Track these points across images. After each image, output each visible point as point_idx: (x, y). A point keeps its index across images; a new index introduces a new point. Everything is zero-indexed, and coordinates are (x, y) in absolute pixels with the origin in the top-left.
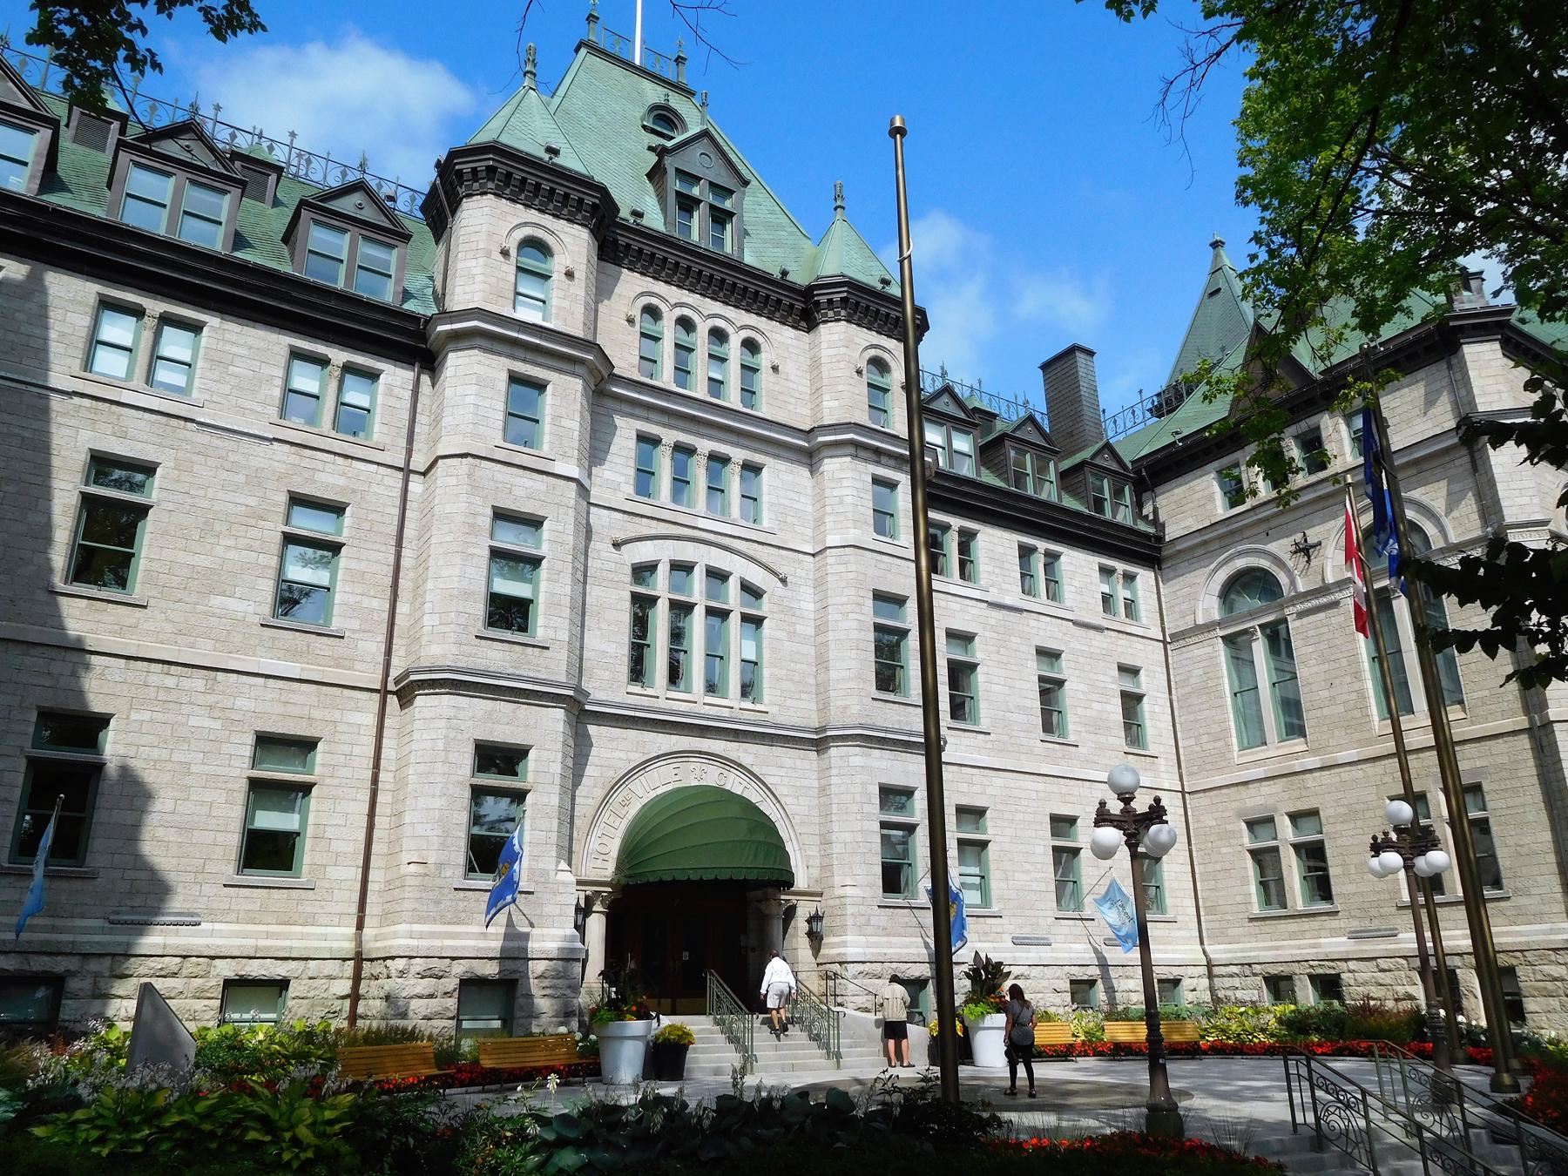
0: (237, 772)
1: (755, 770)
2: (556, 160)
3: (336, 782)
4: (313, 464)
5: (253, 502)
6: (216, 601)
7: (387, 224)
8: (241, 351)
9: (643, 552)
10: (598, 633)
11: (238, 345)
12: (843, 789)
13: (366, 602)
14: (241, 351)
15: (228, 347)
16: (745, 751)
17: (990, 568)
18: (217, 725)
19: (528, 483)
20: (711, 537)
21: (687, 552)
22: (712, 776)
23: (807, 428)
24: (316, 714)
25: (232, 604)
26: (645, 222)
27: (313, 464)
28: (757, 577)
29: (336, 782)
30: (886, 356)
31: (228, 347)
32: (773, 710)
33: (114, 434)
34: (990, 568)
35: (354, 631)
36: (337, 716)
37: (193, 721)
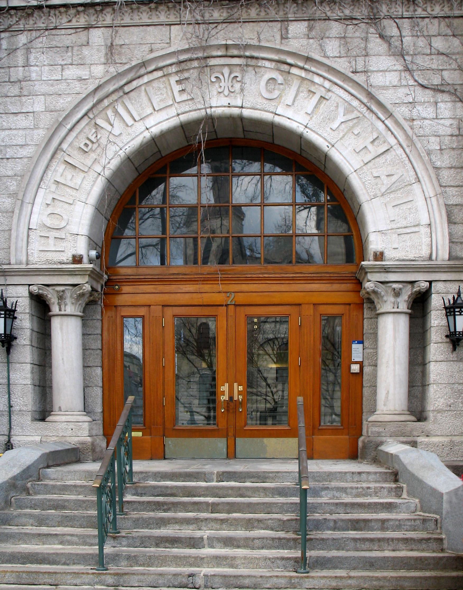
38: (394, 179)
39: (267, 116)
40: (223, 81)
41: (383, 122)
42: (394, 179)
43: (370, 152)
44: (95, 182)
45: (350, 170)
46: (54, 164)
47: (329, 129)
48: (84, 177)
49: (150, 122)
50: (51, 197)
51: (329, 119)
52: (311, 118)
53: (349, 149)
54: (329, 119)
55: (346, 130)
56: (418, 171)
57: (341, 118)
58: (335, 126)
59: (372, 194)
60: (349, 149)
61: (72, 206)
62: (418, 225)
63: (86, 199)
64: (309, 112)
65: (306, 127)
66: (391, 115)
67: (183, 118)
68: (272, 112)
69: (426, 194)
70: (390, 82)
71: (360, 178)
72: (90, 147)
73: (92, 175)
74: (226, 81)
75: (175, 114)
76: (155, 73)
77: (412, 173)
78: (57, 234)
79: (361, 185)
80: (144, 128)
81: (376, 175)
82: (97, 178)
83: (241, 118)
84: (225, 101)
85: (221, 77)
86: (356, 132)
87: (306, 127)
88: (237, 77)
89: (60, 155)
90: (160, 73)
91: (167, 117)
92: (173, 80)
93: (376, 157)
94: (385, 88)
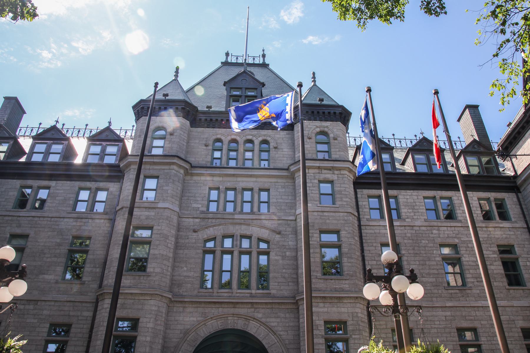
0: (41, 338)
1: (263, 320)
2: (167, 98)
3: (76, 339)
4: (81, 224)
5: (58, 241)
6: (41, 277)
7: (117, 138)
8: (62, 191)
9: (210, 232)
10: (185, 269)
11: (60, 190)
13: (94, 270)
14: (62, 191)
15: (57, 191)
16: (258, 312)
17: (406, 210)
18: (36, 321)
19: (147, 213)
20: (242, 221)
21: (231, 229)
22: (240, 325)
23: (287, 168)
24: (71, 313)
25: (46, 277)
26: (212, 109)
27: (81, 224)
28: (265, 234)
29: (76, 339)
30: (326, 129)
31: (57, 191)
32: (273, 292)
33: (17, 227)
34: (406, 210)
35: (89, 281)
36: (79, 314)
37: (28, 321)
46: (184, 344)
66: (275, 334)
92: (219, 322)
94: (274, 326)
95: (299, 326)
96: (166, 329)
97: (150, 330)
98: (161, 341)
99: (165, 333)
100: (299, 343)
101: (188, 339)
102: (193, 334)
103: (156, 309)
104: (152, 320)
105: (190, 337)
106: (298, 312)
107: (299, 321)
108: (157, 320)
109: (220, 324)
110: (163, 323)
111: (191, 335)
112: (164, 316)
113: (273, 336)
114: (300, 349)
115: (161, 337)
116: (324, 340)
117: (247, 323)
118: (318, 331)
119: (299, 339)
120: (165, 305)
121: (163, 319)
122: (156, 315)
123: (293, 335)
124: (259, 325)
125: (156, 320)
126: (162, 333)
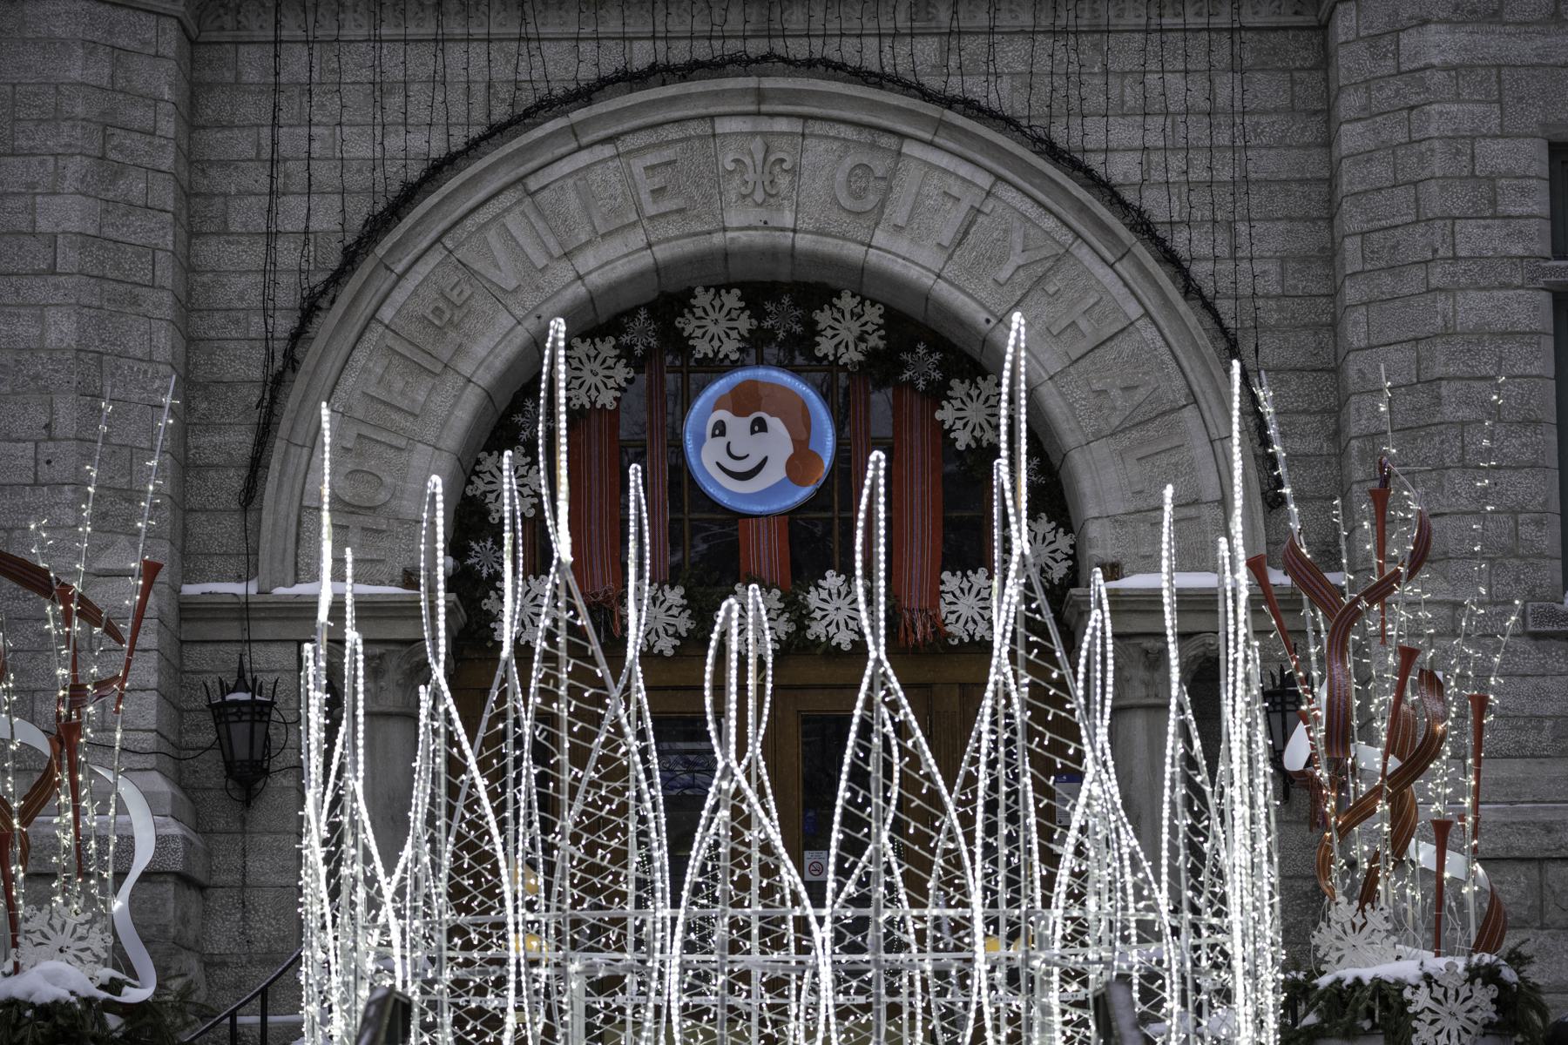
12: (1380, 171)
38: (1139, 395)
39: (853, 251)
40: (751, 169)
41: (1112, 266)
42: (1139, 395)
43: (1084, 336)
44: (458, 398)
45: (1040, 376)
46: (360, 356)
47: (989, 282)
48: (434, 387)
49: (587, 261)
50: (352, 431)
51: (990, 259)
52: (950, 257)
53: (1037, 327)
54: (990, 259)
55: (1028, 285)
56: (1191, 377)
57: (1017, 259)
58: (1003, 275)
59: (1089, 430)
60: (1037, 327)
61: (405, 454)
62: (1196, 502)
63: (438, 438)
64: (946, 243)
65: (939, 276)
67: (663, 253)
68: (863, 244)
69: (1213, 430)
70: (1125, 174)
71: (1062, 394)
72: (447, 316)
73: (451, 383)
74: (759, 169)
75: (643, 244)
76: (597, 148)
77: (1179, 382)
78: (368, 521)
79: (1066, 410)
80: (572, 275)
81: (1097, 386)
82: (463, 389)
83: (792, 252)
84: (754, 216)
85: (747, 160)
86: (1051, 290)
87: (939, 276)
88: (782, 161)
89: (372, 336)
90: (608, 150)
91: (626, 251)
92: (638, 165)
93: (1097, 347)
95: (1331, 182)
96: (193, 234)
97: (69, 258)
98: (164, 342)
99: (188, 267)
100: (1334, 326)
101: (387, 314)
102: (423, 269)
103: (100, 72)
104: (75, 166)
105: (399, 296)
106: (1324, 61)
107: (1328, 143)
108: (119, 171)
109: (645, 186)
110: (166, 195)
111: (410, 284)
112: (168, 126)
113: (1101, 271)
114: (1335, 371)
115: (162, 304)
116: (1545, 299)
117: (880, 166)
118: (1497, 229)
119: (1334, 295)
120: (170, 40)
121: (167, 161)
122: (107, 125)
123: (1283, 260)
124: (984, 180)
125: (108, 168)
126: (166, 273)
